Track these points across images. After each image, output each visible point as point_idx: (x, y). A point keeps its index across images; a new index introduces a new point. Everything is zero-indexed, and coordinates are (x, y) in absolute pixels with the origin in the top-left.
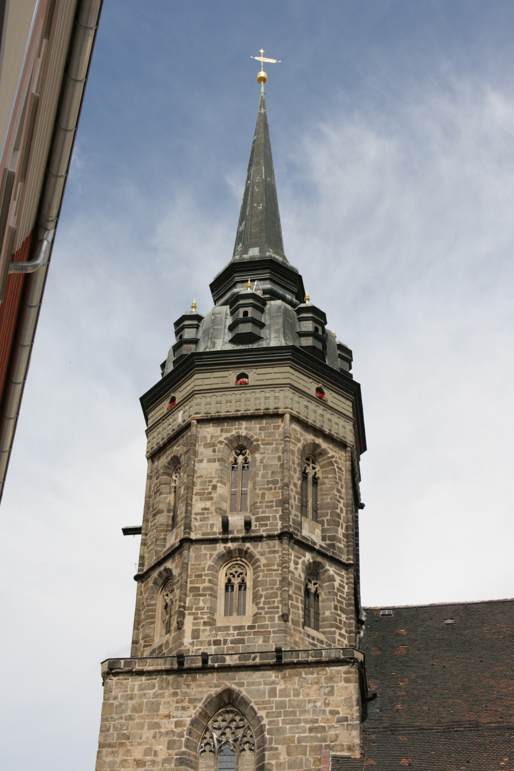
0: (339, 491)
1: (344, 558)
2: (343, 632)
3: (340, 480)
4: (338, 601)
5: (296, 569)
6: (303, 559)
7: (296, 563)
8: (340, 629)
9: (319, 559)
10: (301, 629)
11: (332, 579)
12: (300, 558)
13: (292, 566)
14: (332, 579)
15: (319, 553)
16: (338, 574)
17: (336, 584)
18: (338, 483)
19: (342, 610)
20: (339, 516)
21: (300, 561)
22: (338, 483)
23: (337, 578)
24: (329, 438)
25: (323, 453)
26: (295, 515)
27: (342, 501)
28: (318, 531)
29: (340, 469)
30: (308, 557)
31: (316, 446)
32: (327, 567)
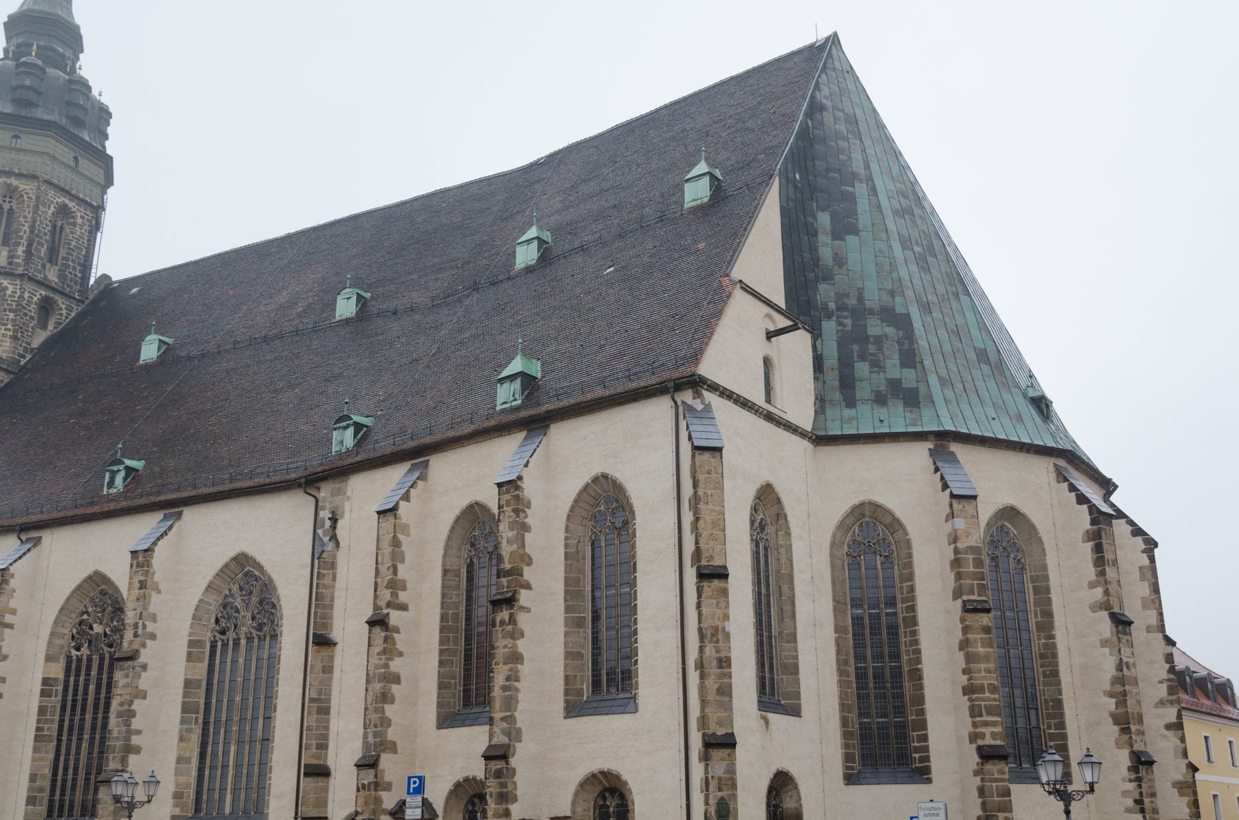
0: (25, 217)
1: (20, 270)
3: (28, 206)
11: (6, 288)
14: (6, 288)
17: (8, 293)
20: (21, 237)
23: (11, 288)
24: (20, 175)
25: (17, 188)
31: (10, 185)
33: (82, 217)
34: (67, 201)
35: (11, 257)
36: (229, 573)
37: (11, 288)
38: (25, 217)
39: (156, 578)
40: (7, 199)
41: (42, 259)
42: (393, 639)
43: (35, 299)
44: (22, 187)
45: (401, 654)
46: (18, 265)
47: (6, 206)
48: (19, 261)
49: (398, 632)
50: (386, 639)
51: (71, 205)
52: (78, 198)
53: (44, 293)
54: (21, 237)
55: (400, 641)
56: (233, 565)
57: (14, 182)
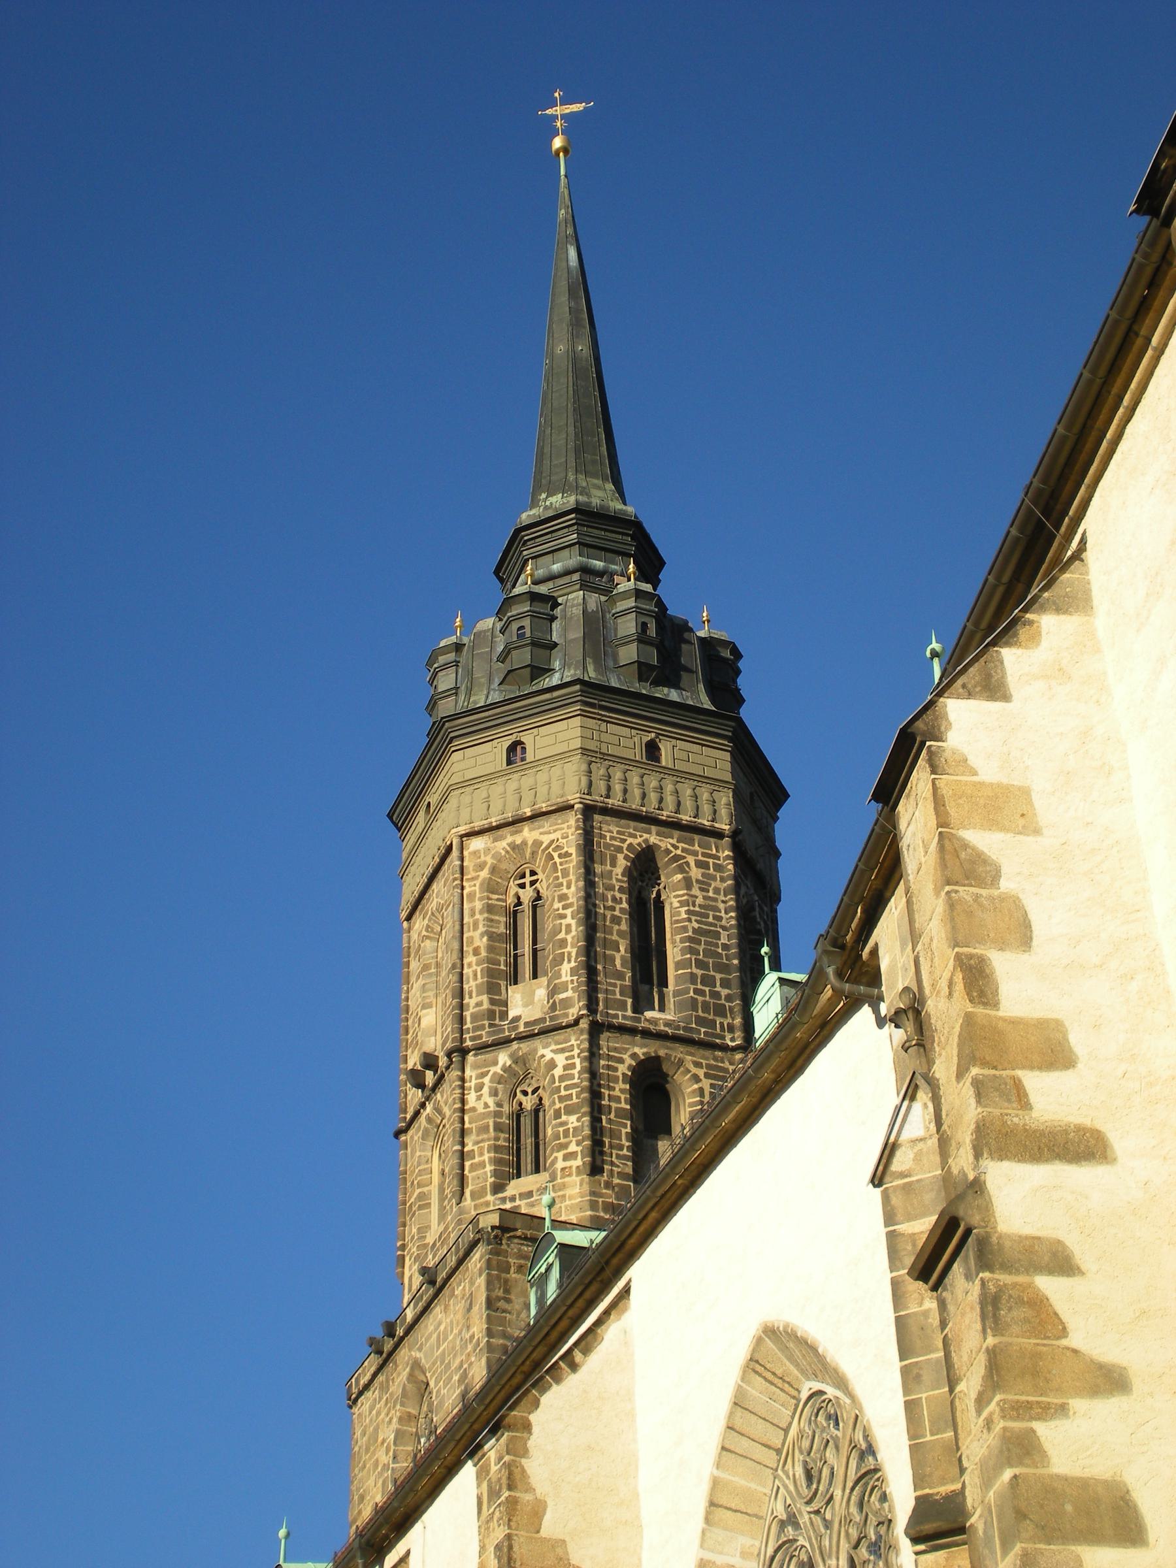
2: (573, 1147)
4: (561, 1099)
5: (479, 1098)
6: (493, 1069)
7: (479, 1088)
8: (566, 1146)
9: (524, 1047)
10: (490, 1198)
12: (483, 1075)
13: (471, 1098)
14: (552, 1065)
15: (521, 1038)
16: (562, 1050)
17: (558, 1072)
18: (561, 884)
19: (570, 1111)
21: (486, 1080)
22: (561, 884)
23: (561, 1060)
26: (478, 1004)
27: (568, 912)
28: (541, 993)
29: (567, 855)
30: (504, 1057)
32: (541, 1052)
33: (699, 864)
34: (653, 839)
35: (553, 992)
36: (758, 1429)
37: (561, 1060)
38: (563, 897)
39: (550, 1527)
40: (528, 879)
41: (620, 976)
42: (1039, 1304)
43: (622, 1069)
44: (546, 840)
45: (1110, 1380)
46: (566, 1003)
47: (527, 895)
48: (569, 993)
49: (1062, 1263)
50: (992, 1308)
51: (665, 843)
52: (676, 825)
53: (640, 1051)
54: (563, 943)
55: (1086, 1309)
56: (757, 1390)
57: (528, 834)
